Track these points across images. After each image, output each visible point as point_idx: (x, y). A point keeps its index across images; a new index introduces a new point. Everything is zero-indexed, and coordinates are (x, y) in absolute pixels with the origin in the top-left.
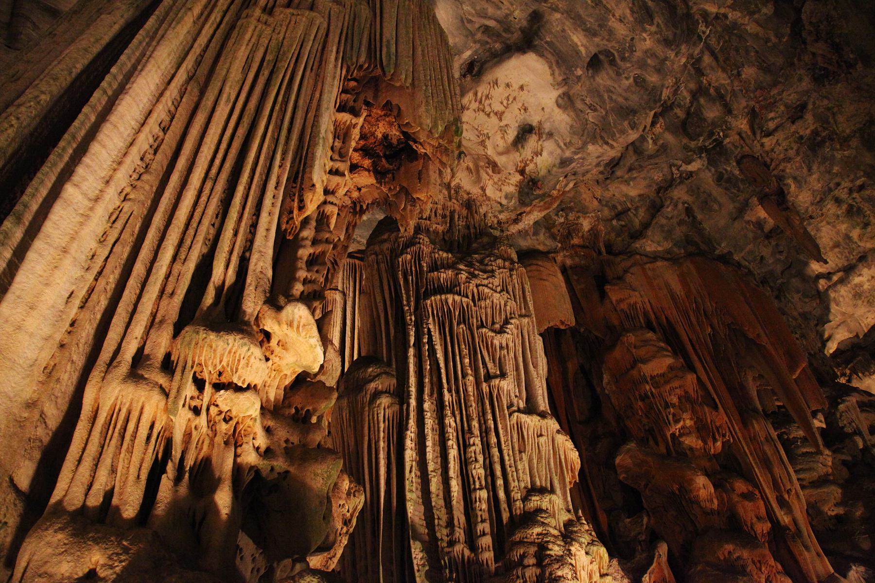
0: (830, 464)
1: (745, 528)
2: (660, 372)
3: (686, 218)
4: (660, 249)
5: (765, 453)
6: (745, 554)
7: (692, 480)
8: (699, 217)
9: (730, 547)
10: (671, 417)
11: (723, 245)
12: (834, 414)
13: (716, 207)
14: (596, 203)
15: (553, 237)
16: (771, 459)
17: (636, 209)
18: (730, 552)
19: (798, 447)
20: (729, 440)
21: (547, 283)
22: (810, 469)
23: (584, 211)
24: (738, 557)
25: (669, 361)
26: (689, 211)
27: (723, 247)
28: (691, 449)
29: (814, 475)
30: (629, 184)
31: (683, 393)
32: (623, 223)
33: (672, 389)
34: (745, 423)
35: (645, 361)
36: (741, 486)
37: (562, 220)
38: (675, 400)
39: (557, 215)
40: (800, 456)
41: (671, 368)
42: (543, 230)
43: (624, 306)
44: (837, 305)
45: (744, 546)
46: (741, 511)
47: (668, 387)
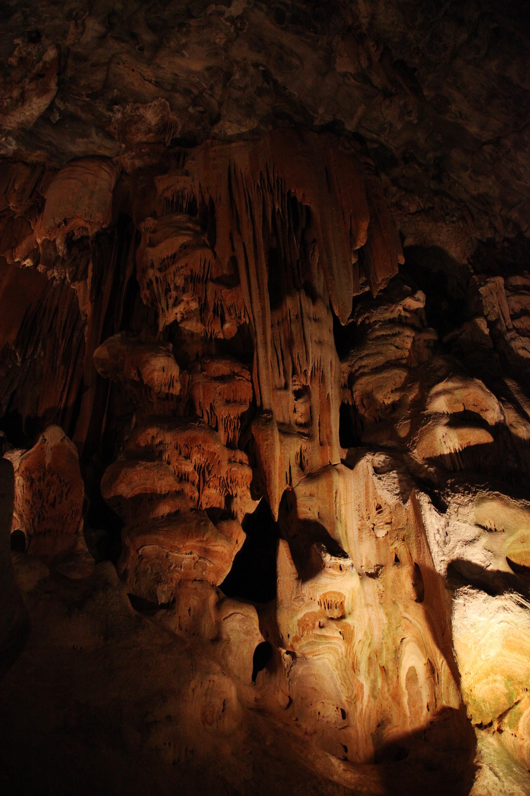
0: (409, 346)
1: (198, 412)
2: (170, 254)
3: (266, 85)
4: (244, 130)
5: (291, 334)
6: (168, 438)
7: (147, 361)
8: (280, 80)
9: (153, 431)
10: (171, 302)
11: (321, 111)
12: (481, 301)
13: (295, 61)
14: (151, 88)
15: (110, 136)
16: (295, 337)
17: (211, 88)
18: (153, 437)
19: (374, 330)
20: (246, 322)
21: (73, 181)
22: (378, 353)
23: (140, 100)
24: (161, 443)
25: (183, 240)
26: (266, 75)
27: (322, 115)
28: (192, 334)
29: (381, 360)
30: (183, 56)
31: (189, 273)
32: (201, 109)
33: (178, 270)
34: (276, 303)
35: (152, 244)
36: (222, 367)
37: (119, 116)
38: (180, 281)
39: (112, 111)
40: (373, 340)
41: (184, 247)
42: (93, 130)
43: (168, 194)
44: (519, 179)
45: (169, 430)
46: (199, 393)
47: (173, 269)
